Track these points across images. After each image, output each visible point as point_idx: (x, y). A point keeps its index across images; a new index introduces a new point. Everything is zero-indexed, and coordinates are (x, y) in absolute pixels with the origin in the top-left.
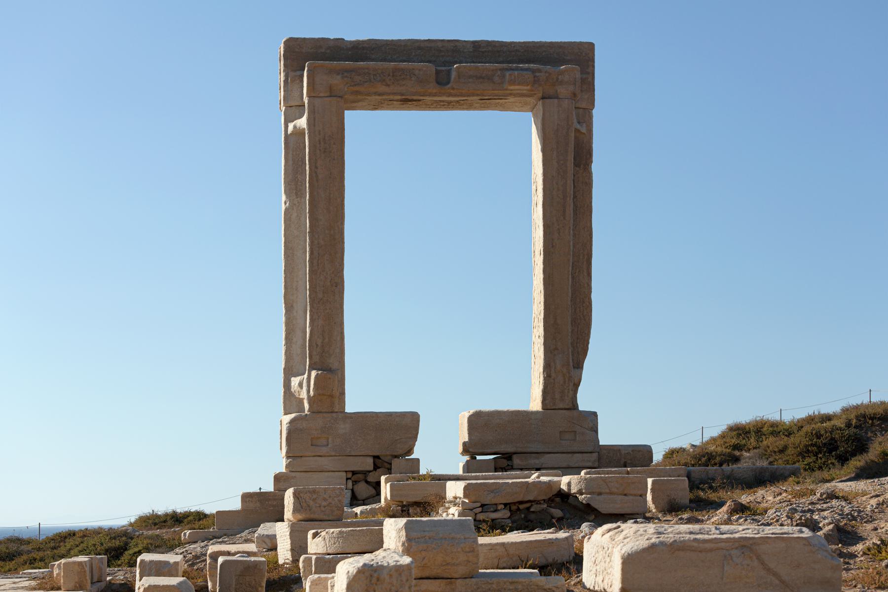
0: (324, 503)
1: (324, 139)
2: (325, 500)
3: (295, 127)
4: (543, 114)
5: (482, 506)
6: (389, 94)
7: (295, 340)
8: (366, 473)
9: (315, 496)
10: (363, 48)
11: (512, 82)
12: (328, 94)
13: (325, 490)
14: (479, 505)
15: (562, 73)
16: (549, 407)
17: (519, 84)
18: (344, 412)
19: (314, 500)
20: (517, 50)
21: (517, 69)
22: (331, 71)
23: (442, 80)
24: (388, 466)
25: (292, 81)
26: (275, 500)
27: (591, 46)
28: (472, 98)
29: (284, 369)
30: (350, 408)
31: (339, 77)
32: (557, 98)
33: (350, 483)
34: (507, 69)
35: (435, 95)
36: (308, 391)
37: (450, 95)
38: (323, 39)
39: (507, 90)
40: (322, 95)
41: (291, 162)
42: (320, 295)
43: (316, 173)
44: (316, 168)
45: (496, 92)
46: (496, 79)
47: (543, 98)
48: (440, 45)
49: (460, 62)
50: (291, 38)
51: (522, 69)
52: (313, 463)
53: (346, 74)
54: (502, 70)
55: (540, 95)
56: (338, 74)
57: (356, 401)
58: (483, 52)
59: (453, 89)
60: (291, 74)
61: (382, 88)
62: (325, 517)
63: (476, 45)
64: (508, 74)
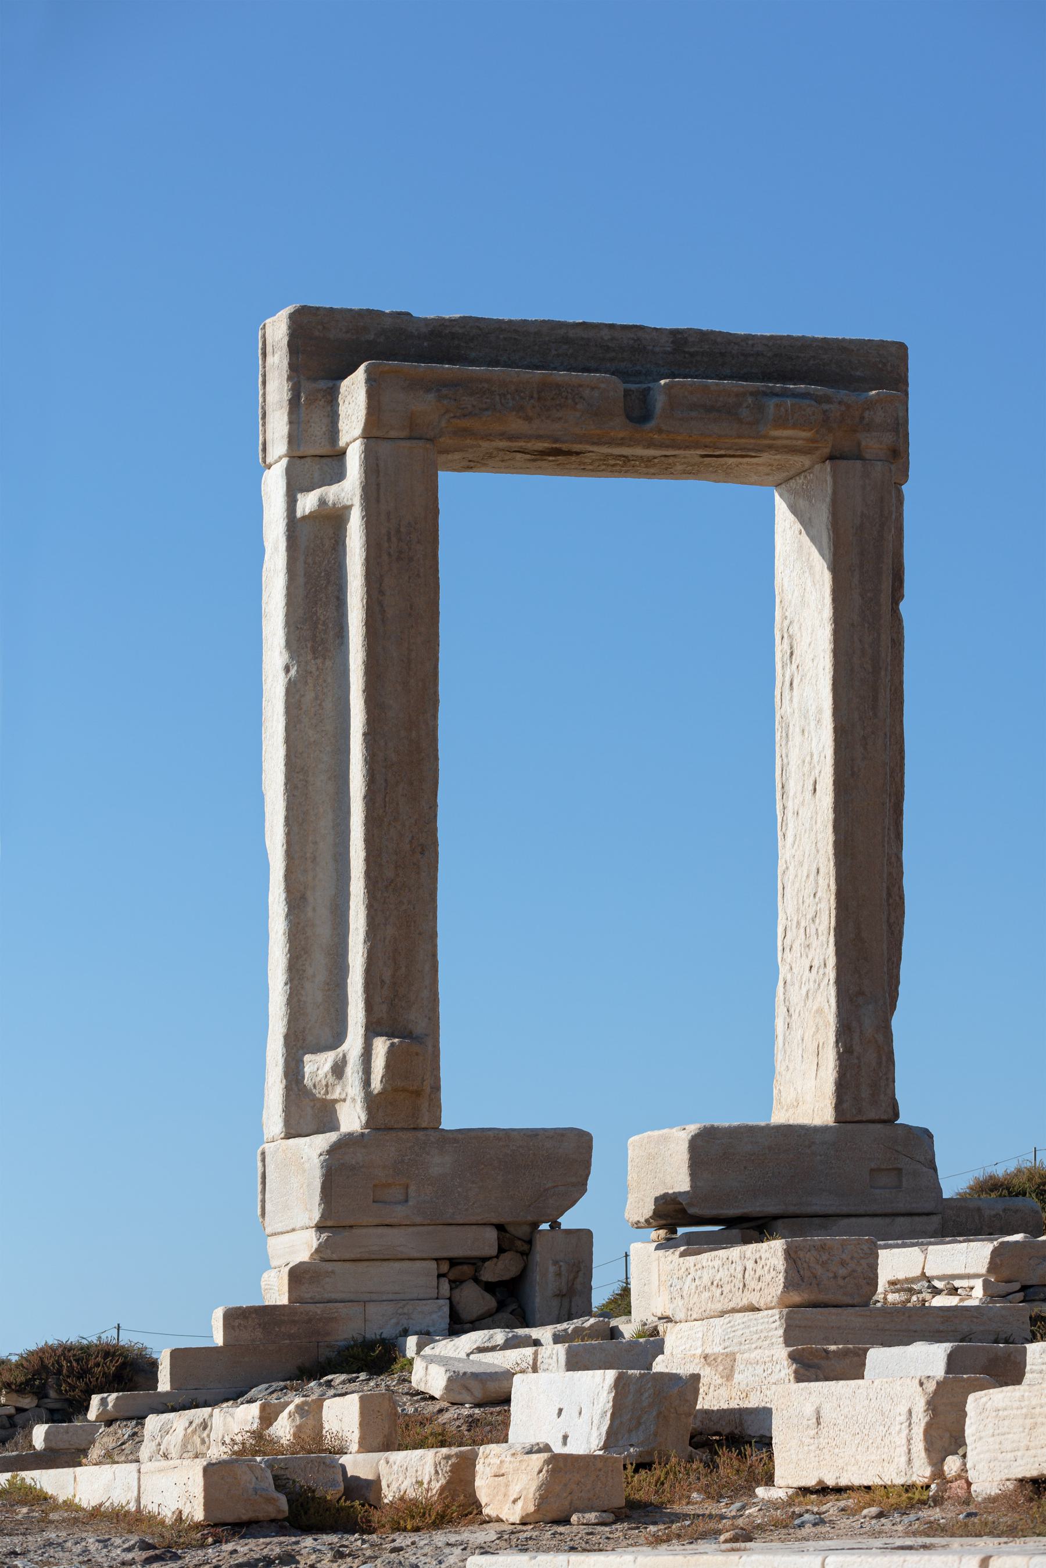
0: (842, 1271)
1: (398, 531)
2: (843, 1263)
3: (322, 502)
4: (835, 493)
5: (1024, 1288)
6: (528, 438)
7: (310, 971)
8: (477, 1262)
9: (825, 1257)
10: (453, 336)
11: (781, 422)
12: (404, 434)
13: (843, 1244)
14: (1017, 1286)
15: (871, 404)
16: (849, 1118)
17: (794, 427)
18: (437, 1129)
19: (824, 1264)
20: (758, 354)
21: (784, 394)
22: (415, 384)
23: (639, 411)
24: (526, 1247)
25: (310, 402)
26: (294, 1322)
27: (901, 349)
28: (687, 453)
29: (286, 1037)
30: (450, 1121)
31: (431, 397)
32: (859, 457)
33: (445, 1286)
34: (775, 394)
35: (622, 443)
36: (367, 1082)
37: (651, 444)
38: (370, 312)
39: (765, 437)
40: (393, 434)
41: (301, 580)
42: (389, 873)
43: (380, 604)
44: (382, 592)
45: (743, 441)
46: (744, 413)
47: (831, 458)
48: (606, 334)
49: (673, 376)
50: (304, 308)
51: (794, 395)
52: (377, 1240)
53: (444, 391)
54: (755, 394)
55: (826, 451)
56: (428, 390)
57: (462, 1108)
58: (692, 355)
59: (660, 431)
60: (307, 386)
61: (516, 425)
62: (847, 1300)
63: (679, 338)
64: (772, 403)
